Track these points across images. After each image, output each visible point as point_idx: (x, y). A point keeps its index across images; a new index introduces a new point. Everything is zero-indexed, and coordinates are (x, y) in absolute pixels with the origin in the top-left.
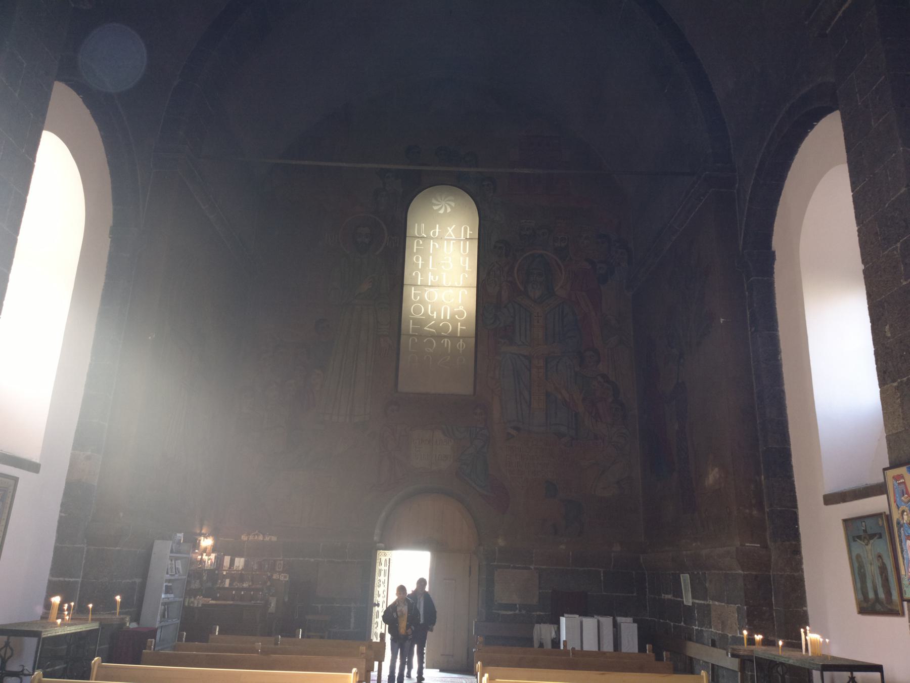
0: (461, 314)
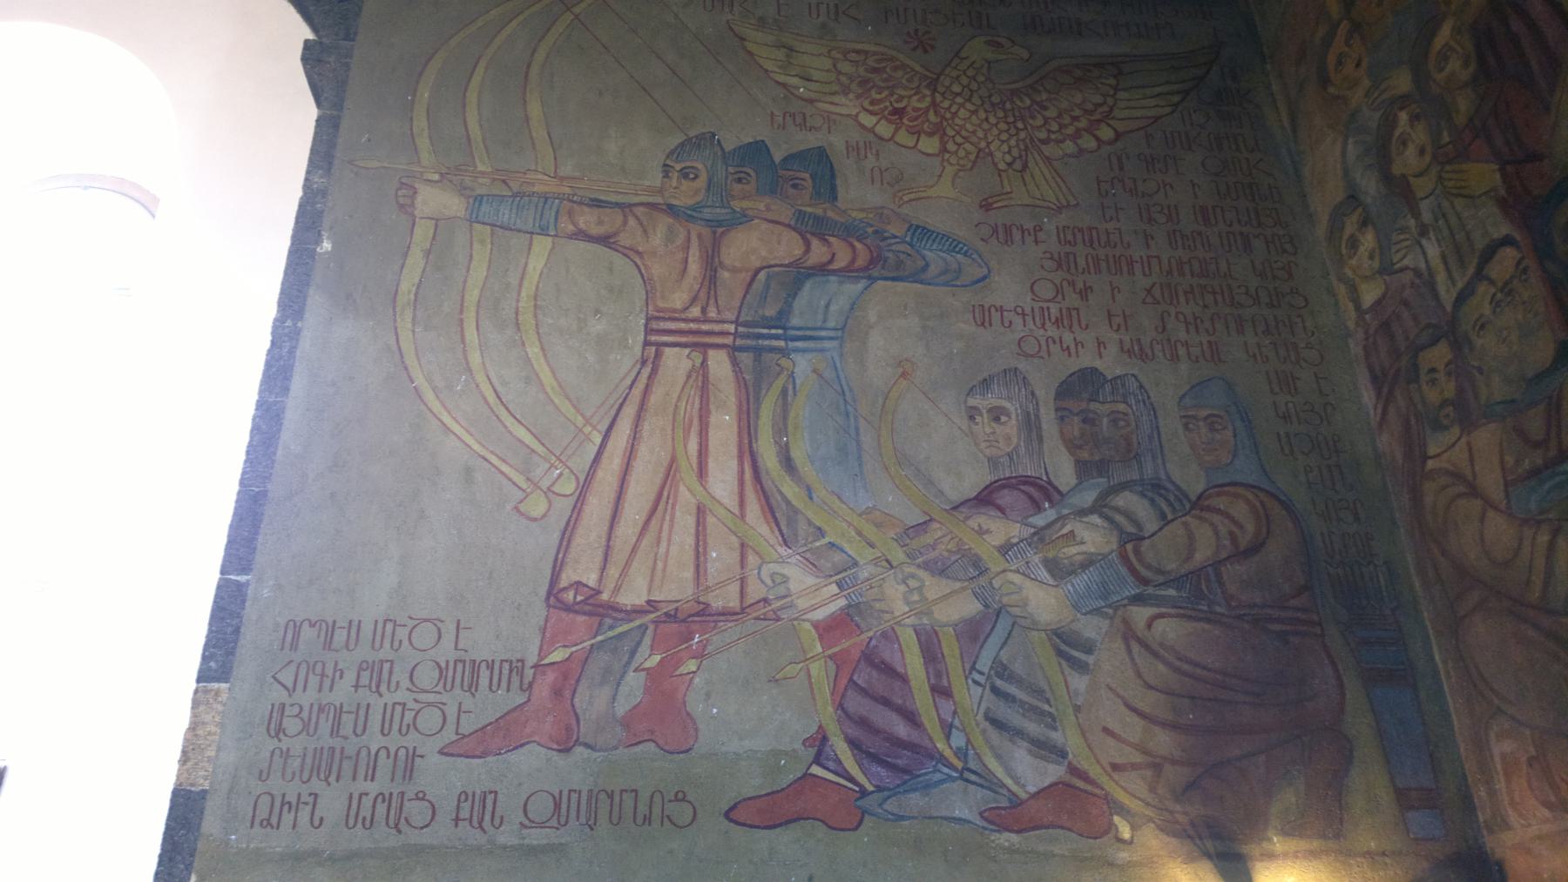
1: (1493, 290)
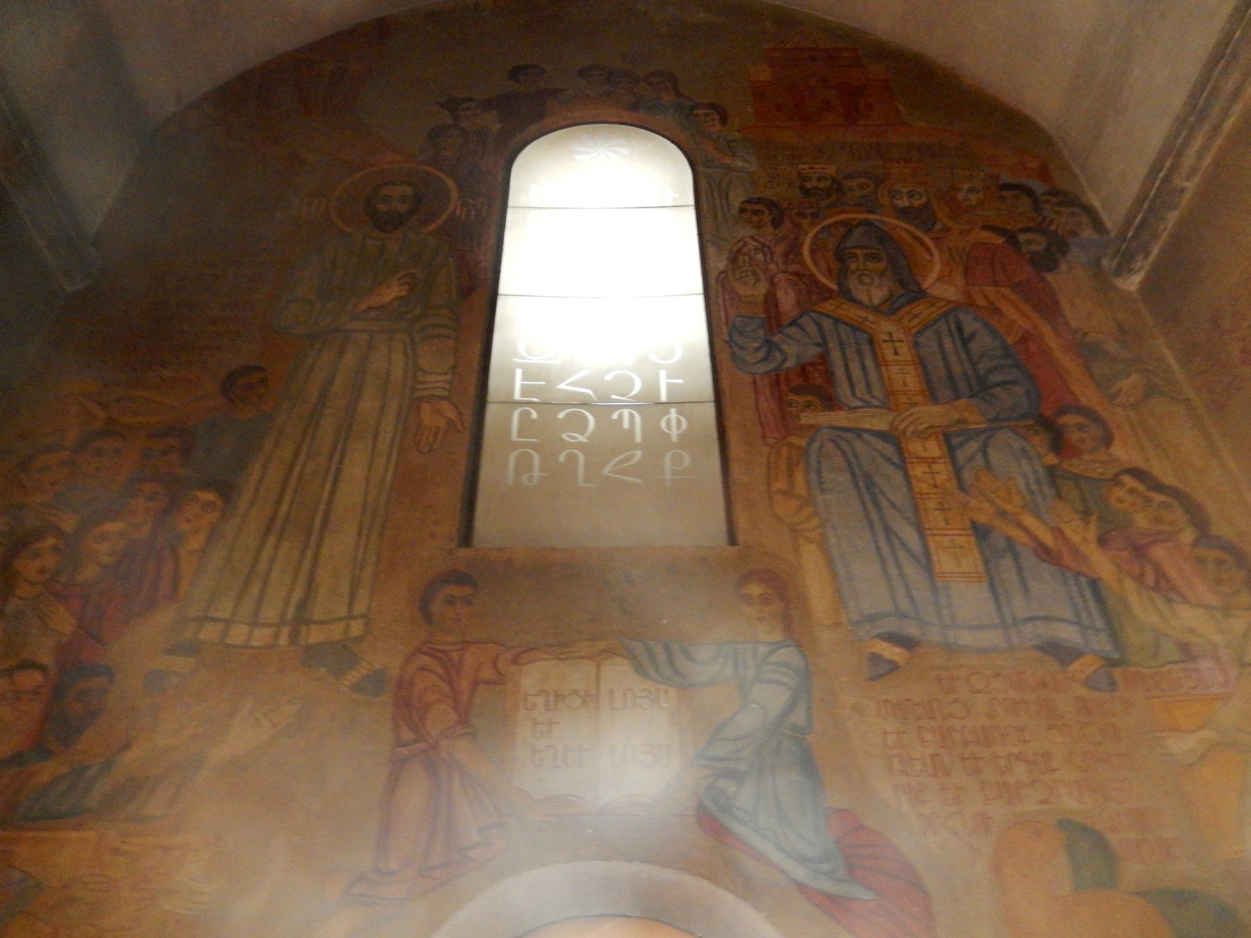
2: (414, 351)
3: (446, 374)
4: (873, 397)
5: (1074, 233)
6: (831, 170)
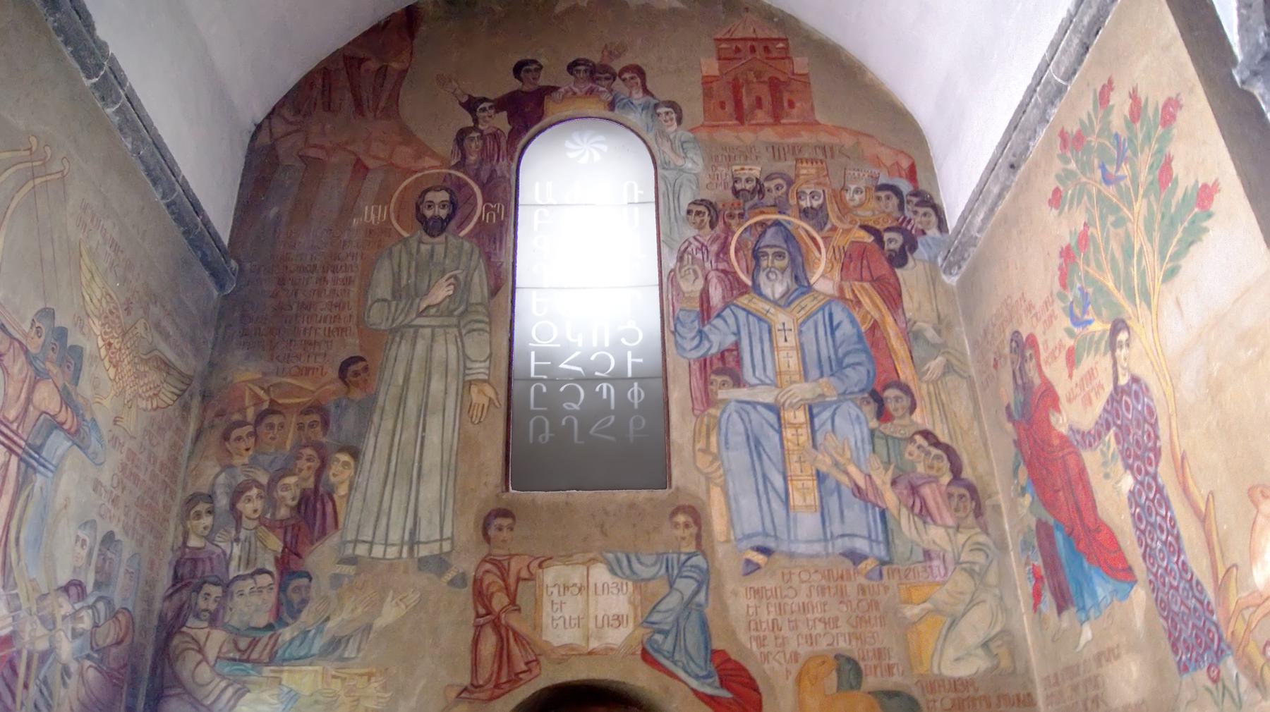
0: (632, 336)
1: (253, 585)
2: (462, 341)
3: (485, 361)
4: (767, 377)
5: (924, 233)
6: (756, 171)
